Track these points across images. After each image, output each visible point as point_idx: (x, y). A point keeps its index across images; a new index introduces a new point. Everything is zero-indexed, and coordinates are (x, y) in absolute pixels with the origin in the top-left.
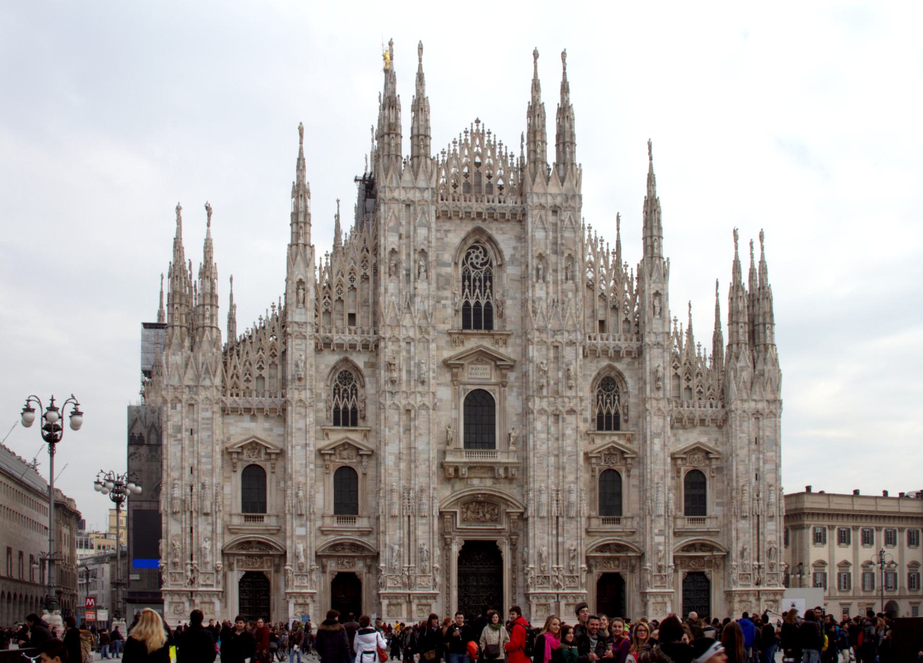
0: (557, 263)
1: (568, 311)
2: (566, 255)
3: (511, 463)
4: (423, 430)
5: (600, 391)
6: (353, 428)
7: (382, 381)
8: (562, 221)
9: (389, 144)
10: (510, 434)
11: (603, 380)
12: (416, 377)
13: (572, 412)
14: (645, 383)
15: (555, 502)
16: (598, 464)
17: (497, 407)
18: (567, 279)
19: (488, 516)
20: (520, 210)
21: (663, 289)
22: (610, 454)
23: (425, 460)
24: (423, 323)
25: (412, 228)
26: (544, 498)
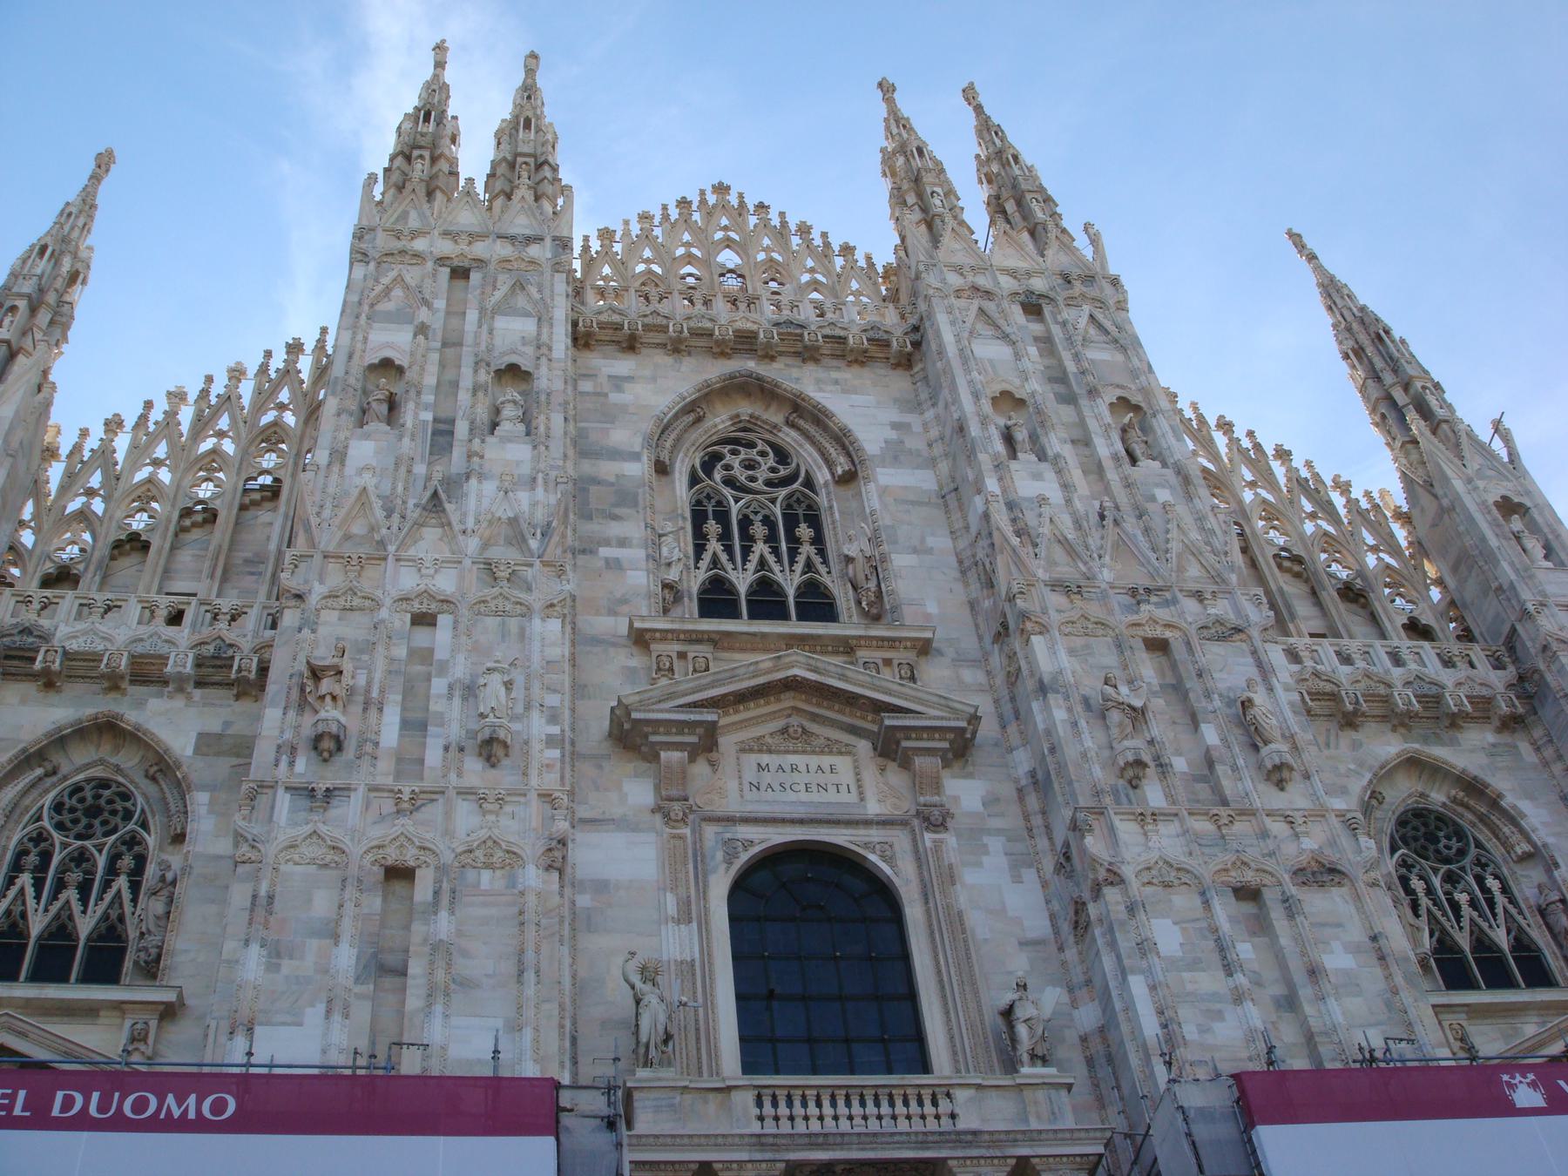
0: (1082, 423)
1: (1174, 534)
2: (1110, 396)
4: (485, 959)
5: (1403, 863)
7: (264, 752)
8: (1064, 324)
10: (1008, 1013)
11: (1402, 823)
12: (455, 731)
13: (1324, 873)
17: (914, 913)
18: (1134, 460)
20: (898, 332)
21: (1528, 493)
24: (502, 553)
25: (472, 316)
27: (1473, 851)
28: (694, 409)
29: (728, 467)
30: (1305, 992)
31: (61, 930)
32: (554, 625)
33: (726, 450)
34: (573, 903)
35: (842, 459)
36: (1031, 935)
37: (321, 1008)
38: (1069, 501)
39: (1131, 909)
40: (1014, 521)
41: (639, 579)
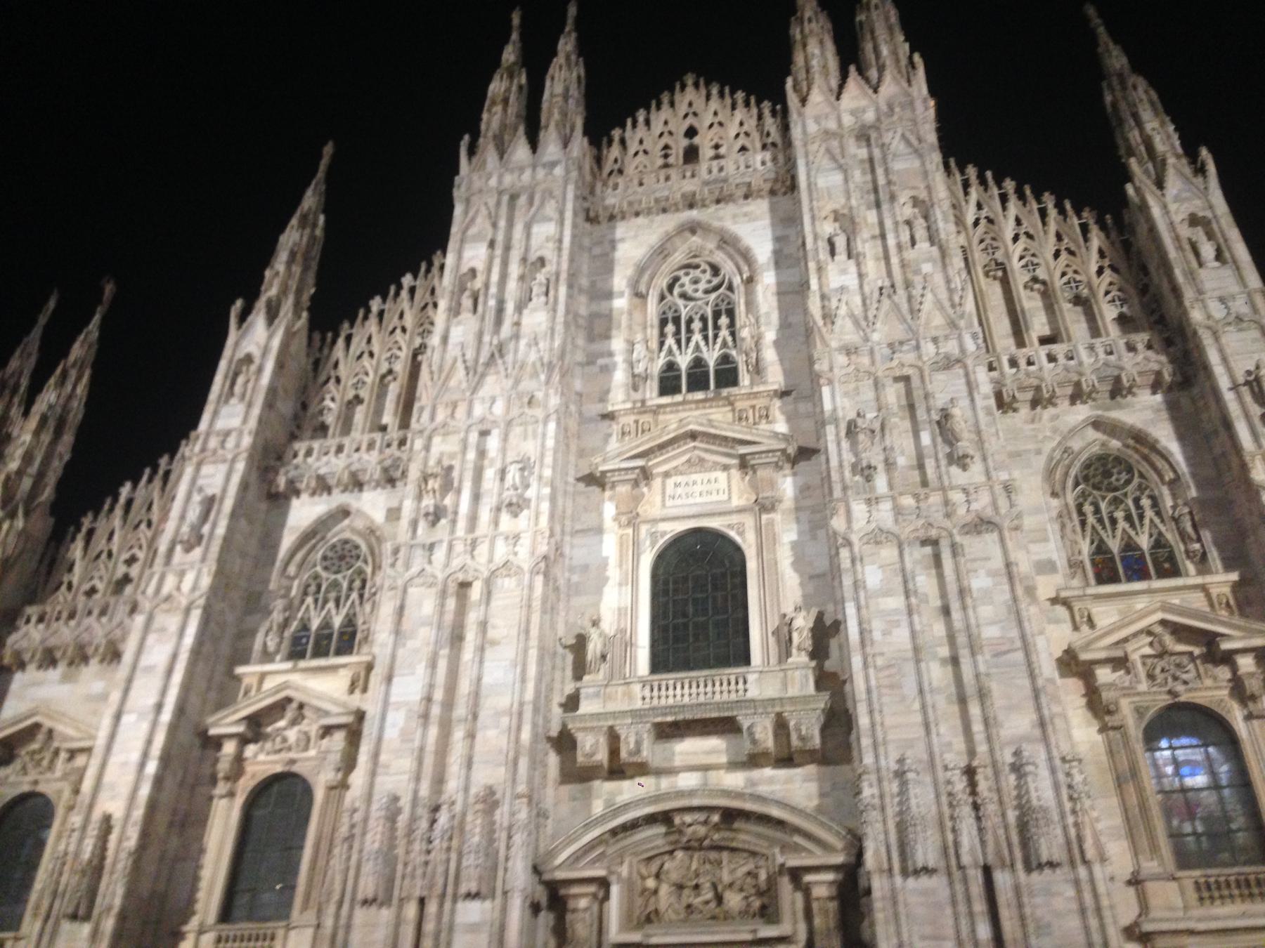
0: (881, 224)
3: (792, 700)
5: (1084, 495)
6: (322, 662)
8: (883, 145)
9: (489, 123)
11: (1087, 466)
13: (981, 525)
14: (1228, 425)
15: (966, 811)
16: (1129, 691)
17: (752, 566)
19: (734, 900)
22: (1163, 654)
23: (498, 714)
24: (527, 385)
26: (922, 799)
27: (1136, 480)
28: (662, 251)
29: (682, 286)
30: (955, 606)
31: (326, 624)
32: (552, 426)
33: (681, 273)
34: (569, 580)
35: (745, 268)
36: (818, 571)
37: (424, 664)
38: (861, 286)
39: (853, 561)
40: (823, 307)
41: (620, 376)
